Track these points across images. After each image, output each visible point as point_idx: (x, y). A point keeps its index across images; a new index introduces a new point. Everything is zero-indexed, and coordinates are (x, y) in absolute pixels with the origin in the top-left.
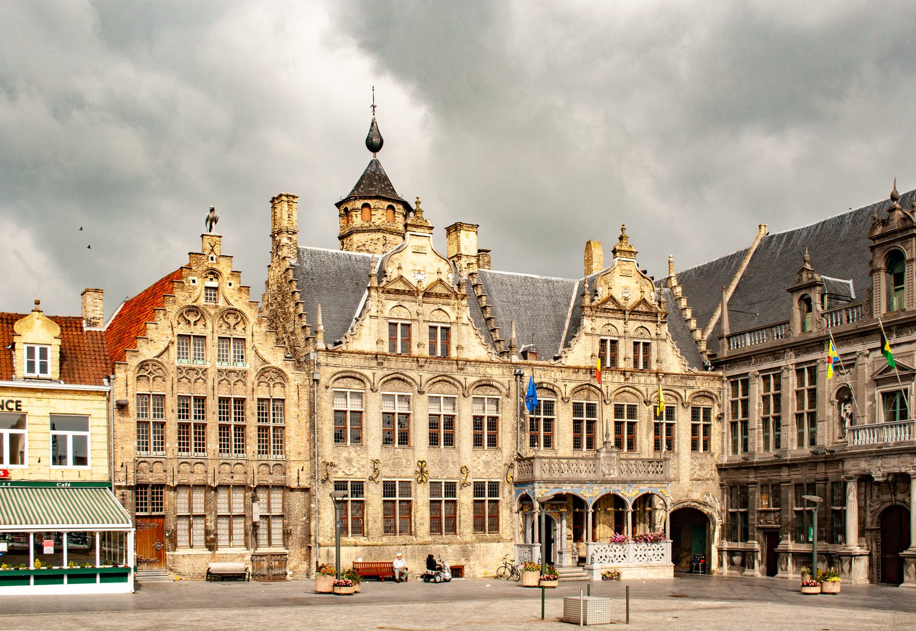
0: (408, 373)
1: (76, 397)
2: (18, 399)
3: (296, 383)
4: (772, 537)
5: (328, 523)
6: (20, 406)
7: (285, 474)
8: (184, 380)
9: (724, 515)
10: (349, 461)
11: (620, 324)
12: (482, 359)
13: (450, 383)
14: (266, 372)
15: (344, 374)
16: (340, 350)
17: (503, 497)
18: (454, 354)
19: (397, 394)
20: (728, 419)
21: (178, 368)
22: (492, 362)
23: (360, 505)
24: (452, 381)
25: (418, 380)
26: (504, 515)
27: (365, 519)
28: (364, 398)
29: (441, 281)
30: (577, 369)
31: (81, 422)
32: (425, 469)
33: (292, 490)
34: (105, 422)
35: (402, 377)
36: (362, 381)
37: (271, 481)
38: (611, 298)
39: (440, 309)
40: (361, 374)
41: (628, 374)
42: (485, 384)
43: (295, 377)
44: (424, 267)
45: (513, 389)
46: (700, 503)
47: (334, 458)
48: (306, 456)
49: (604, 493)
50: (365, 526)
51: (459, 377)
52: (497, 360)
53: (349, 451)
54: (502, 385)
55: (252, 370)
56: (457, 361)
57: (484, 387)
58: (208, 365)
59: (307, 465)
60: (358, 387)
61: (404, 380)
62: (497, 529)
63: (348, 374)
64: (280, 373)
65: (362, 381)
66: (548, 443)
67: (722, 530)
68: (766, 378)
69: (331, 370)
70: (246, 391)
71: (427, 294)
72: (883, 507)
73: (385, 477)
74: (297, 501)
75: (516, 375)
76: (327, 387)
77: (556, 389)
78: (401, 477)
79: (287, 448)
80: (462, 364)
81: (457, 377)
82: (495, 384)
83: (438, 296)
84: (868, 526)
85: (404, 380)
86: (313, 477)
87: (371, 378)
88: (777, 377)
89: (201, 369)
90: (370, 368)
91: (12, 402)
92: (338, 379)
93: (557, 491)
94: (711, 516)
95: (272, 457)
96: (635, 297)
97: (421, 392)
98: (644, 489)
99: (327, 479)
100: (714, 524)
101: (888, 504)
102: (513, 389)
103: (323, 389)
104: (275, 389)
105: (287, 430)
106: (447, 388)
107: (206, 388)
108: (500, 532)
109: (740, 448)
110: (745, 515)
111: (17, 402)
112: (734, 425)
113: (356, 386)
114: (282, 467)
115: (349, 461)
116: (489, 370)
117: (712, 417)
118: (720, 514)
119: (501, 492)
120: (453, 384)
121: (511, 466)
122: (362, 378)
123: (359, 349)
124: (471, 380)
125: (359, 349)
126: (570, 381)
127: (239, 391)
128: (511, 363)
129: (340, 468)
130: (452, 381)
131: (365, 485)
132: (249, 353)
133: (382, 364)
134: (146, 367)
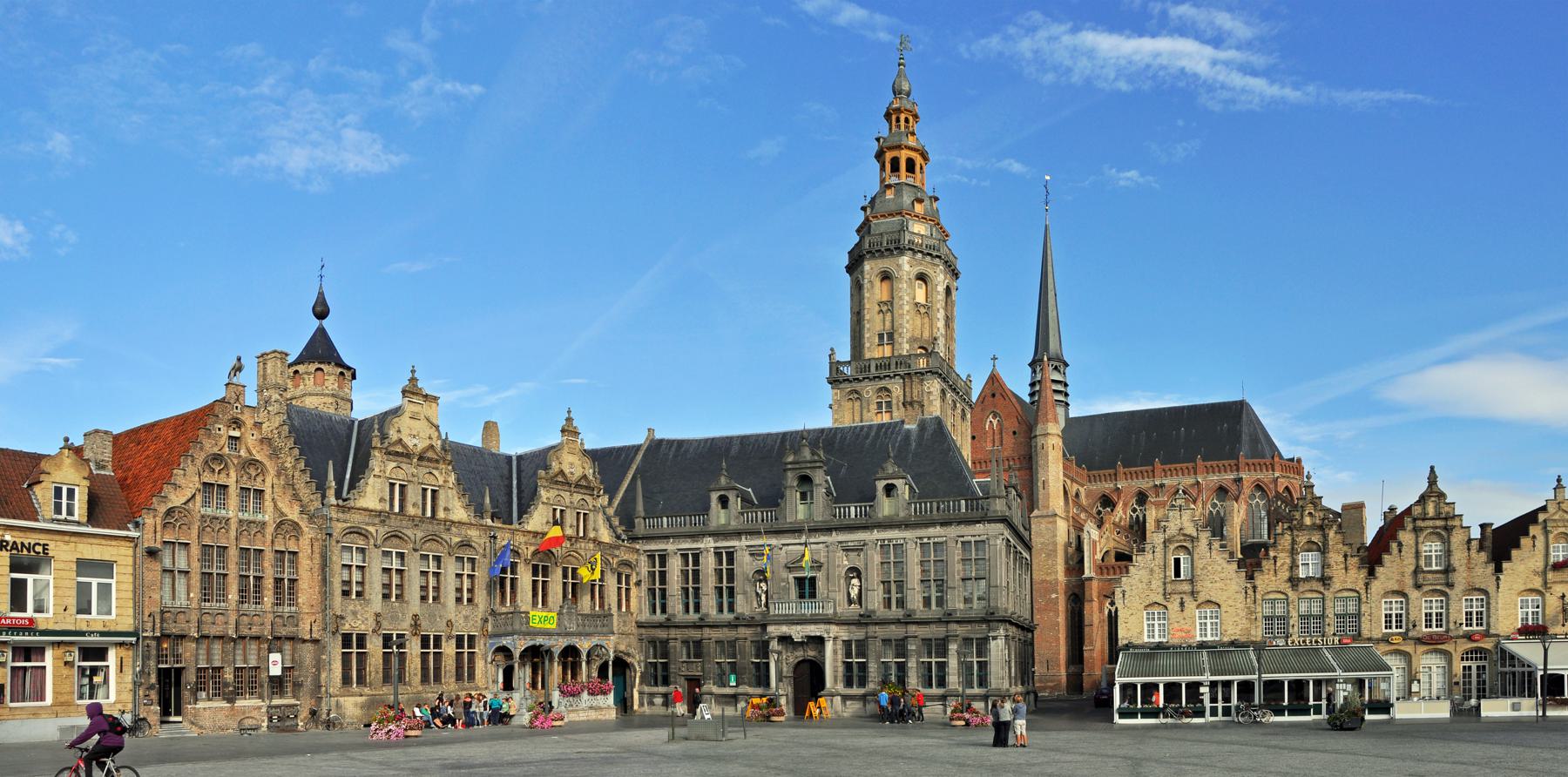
0: (404, 531)
1: (103, 542)
2: (45, 542)
3: (310, 536)
4: (694, 682)
5: (337, 674)
6: (47, 549)
7: (297, 626)
8: (208, 529)
9: (642, 665)
10: (354, 613)
12: (463, 521)
13: (438, 542)
14: (286, 527)
15: (352, 530)
16: (349, 506)
17: (480, 650)
18: (441, 514)
19: (394, 551)
20: (644, 587)
21: (203, 516)
22: (471, 524)
23: (362, 657)
24: (439, 539)
25: (413, 538)
26: (480, 665)
27: (368, 669)
28: (367, 554)
29: (432, 447)
30: (536, 534)
31: (105, 568)
32: (418, 622)
33: (304, 641)
34: (130, 570)
35: (400, 534)
36: (367, 537)
37: (284, 633)
39: (430, 473)
40: (367, 531)
41: (574, 540)
42: (466, 544)
43: (308, 532)
44: (419, 432)
45: (488, 550)
46: (625, 654)
47: (342, 611)
48: (318, 608)
49: (566, 644)
50: (368, 677)
52: (475, 523)
53: (353, 604)
54: (480, 545)
55: (272, 522)
56: (445, 521)
57: (464, 547)
58: (231, 514)
59: (319, 617)
60: (362, 543)
61: (400, 538)
62: (474, 678)
63: (355, 530)
64: (295, 525)
65: (367, 537)
67: (641, 677)
68: (685, 556)
69: (341, 525)
70: (264, 543)
72: (797, 661)
73: (385, 630)
74: (307, 652)
75: (491, 537)
76: (338, 542)
77: (520, 551)
78: (397, 630)
79: (300, 600)
81: (444, 537)
82: (473, 544)
83: (430, 460)
84: (784, 674)
85: (400, 538)
86: (324, 629)
87: (375, 534)
88: (696, 558)
89: (224, 518)
90: (374, 525)
91: (39, 544)
92: (347, 533)
93: (531, 643)
94: (633, 665)
95: (287, 609)
97: (415, 550)
99: (337, 630)
100: (635, 671)
101: (801, 659)
102: (488, 550)
103: (334, 543)
104: (291, 542)
105: (300, 582)
106: (434, 545)
107: (228, 538)
108: (477, 682)
109: (658, 611)
110: (665, 666)
111: (44, 545)
112: (652, 591)
113: (361, 543)
114: (294, 619)
115: (354, 613)
116: (468, 531)
117: (631, 583)
118: (639, 663)
119: (477, 645)
120: (441, 543)
121: (486, 621)
122: (367, 534)
123: (365, 506)
125: (364, 506)
126: (531, 544)
127: (257, 542)
128: (486, 526)
129: (347, 621)
130: (439, 539)
131: (368, 637)
132: (268, 504)
133: (384, 521)
134: (173, 514)
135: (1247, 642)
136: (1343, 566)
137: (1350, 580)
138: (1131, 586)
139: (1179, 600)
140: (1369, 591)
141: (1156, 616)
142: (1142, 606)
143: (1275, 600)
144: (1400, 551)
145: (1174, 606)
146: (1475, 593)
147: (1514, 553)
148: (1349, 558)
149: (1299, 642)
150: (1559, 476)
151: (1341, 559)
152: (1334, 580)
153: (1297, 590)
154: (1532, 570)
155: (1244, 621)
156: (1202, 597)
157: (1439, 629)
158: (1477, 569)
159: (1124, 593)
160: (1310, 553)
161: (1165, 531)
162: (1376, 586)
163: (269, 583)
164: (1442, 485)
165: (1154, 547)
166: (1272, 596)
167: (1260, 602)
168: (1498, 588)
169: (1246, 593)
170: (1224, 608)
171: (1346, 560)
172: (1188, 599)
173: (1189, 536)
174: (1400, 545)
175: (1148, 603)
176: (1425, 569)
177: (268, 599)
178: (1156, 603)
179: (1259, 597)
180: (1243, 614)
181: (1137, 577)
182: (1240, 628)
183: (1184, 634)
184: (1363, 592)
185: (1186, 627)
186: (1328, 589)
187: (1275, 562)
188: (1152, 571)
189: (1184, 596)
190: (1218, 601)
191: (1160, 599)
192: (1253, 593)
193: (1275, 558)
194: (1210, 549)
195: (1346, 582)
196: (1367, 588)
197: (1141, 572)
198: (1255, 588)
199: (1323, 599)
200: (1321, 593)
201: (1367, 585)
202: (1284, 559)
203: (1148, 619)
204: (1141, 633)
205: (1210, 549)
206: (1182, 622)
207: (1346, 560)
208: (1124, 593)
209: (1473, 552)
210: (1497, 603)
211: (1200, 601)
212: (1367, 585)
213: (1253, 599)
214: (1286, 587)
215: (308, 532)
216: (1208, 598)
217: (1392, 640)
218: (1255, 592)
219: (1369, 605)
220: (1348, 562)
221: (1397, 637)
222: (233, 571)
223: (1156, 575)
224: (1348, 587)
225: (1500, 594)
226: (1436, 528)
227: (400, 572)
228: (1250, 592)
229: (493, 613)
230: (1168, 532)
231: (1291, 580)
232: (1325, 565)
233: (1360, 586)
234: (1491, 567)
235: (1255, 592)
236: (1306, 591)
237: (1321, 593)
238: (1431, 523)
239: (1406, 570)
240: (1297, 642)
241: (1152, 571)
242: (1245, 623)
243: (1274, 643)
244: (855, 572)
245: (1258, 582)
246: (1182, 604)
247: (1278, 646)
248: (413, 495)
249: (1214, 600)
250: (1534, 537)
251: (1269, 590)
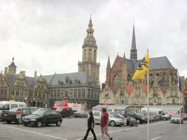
11: (40, 83)
38: (39, 81)
51: (24, 88)
66: (32, 96)
71: (22, 80)
80: (24, 87)
96: (42, 81)
98: (42, 101)
124: (25, 89)
156: (109, 98)
162: (131, 96)
163: (4, 93)
177: (4, 95)
214: (119, 96)
215: (8, 88)
222: (4, 92)
227: (18, 92)
229: (29, 97)
233: (128, 97)
244: (71, 93)
245: (116, 96)
248: (20, 84)
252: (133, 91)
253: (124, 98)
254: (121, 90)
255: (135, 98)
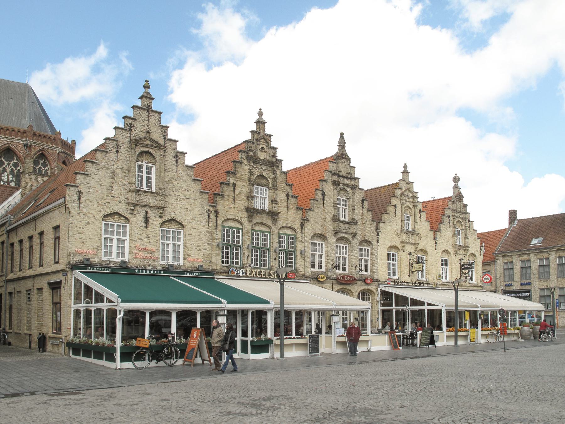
135: (208, 270)
136: (285, 204)
137: (290, 219)
138: (89, 187)
139: (143, 214)
140: (303, 231)
141: (115, 229)
142: (101, 215)
143: (232, 227)
144: (324, 200)
145: (138, 219)
146: (365, 244)
147: (385, 216)
148: (290, 198)
149: (256, 273)
150: (405, 164)
151: (284, 197)
152: (280, 215)
153: (251, 221)
154: (394, 231)
155: (206, 247)
157: (344, 272)
158: (366, 225)
159: (80, 194)
160: (260, 187)
161: (130, 130)
162: (309, 229)
164: (349, 150)
165: (118, 145)
166: (230, 224)
167: (220, 228)
168: (378, 242)
169: (209, 216)
170: (188, 230)
171: (288, 199)
172: (153, 214)
173: (156, 142)
174: (323, 194)
175: (108, 212)
176: (341, 219)
178: (116, 213)
179: (219, 222)
180: (205, 239)
181: (97, 178)
182: (202, 253)
183: (148, 255)
184: (299, 230)
185: (150, 247)
186: (275, 225)
187: (234, 189)
188: (114, 173)
189: (148, 209)
190: (182, 221)
191: (122, 209)
192: (215, 218)
193: (234, 185)
194: (177, 162)
195: (287, 220)
196: (302, 228)
197: (100, 173)
198: (217, 212)
199: (270, 233)
200: (269, 227)
201: (302, 225)
202: (242, 188)
203: (106, 232)
204: (98, 248)
205: (177, 162)
206: (146, 240)
207: (288, 199)
208: (80, 194)
209: (365, 213)
210: (377, 254)
211: (165, 218)
212: (302, 225)
213: (215, 224)
214: (243, 216)
216: (172, 216)
217: (320, 278)
218: (216, 217)
219: (303, 244)
220: (289, 201)
221: (323, 276)
223: (118, 180)
224: (289, 225)
225: (379, 247)
226: (345, 185)
228: (212, 216)
230: (134, 133)
231: (248, 209)
232: (274, 201)
233: (297, 226)
234: (374, 225)
235: (216, 217)
236: (258, 223)
237: (269, 227)
238: (341, 180)
239: (327, 217)
240: (254, 273)
241: (114, 173)
242: (206, 249)
243: (236, 272)
245: (219, 207)
246: (146, 219)
247: (239, 276)
249: (179, 219)
250: (395, 206)
251: (228, 217)
252: (320, 193)
253: (276, 231)
254: (257, 172)
255: (332, 239)
